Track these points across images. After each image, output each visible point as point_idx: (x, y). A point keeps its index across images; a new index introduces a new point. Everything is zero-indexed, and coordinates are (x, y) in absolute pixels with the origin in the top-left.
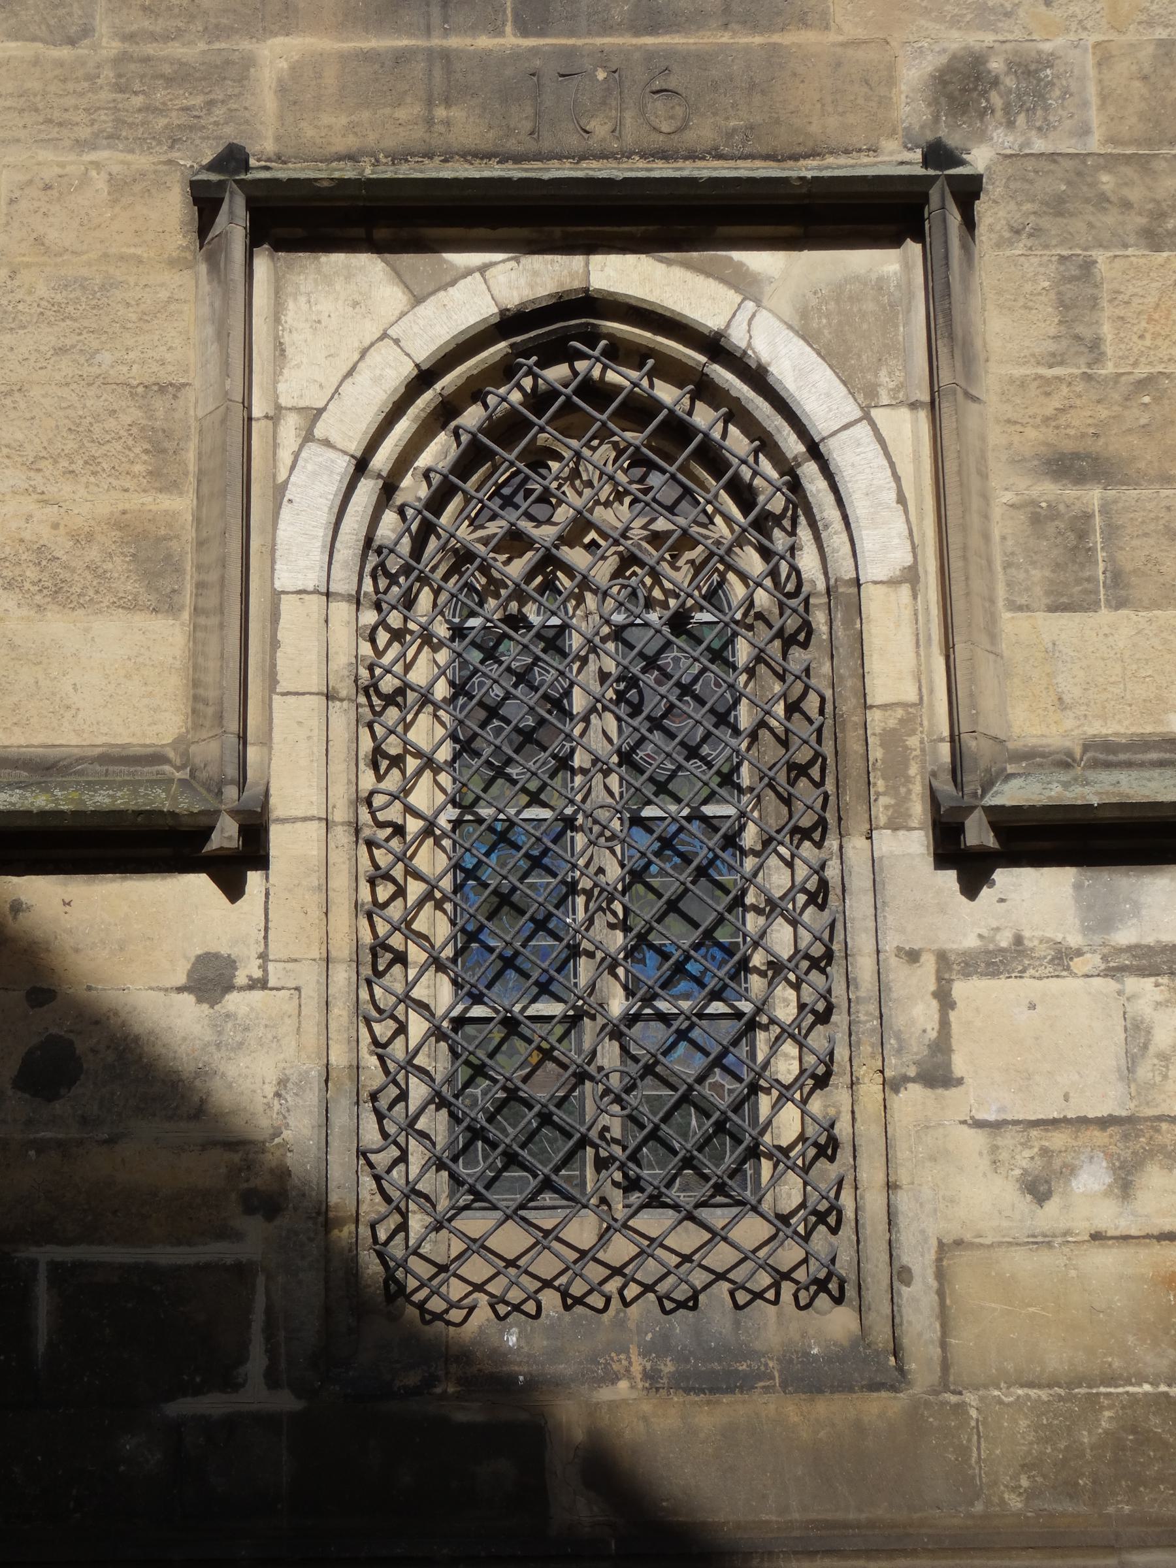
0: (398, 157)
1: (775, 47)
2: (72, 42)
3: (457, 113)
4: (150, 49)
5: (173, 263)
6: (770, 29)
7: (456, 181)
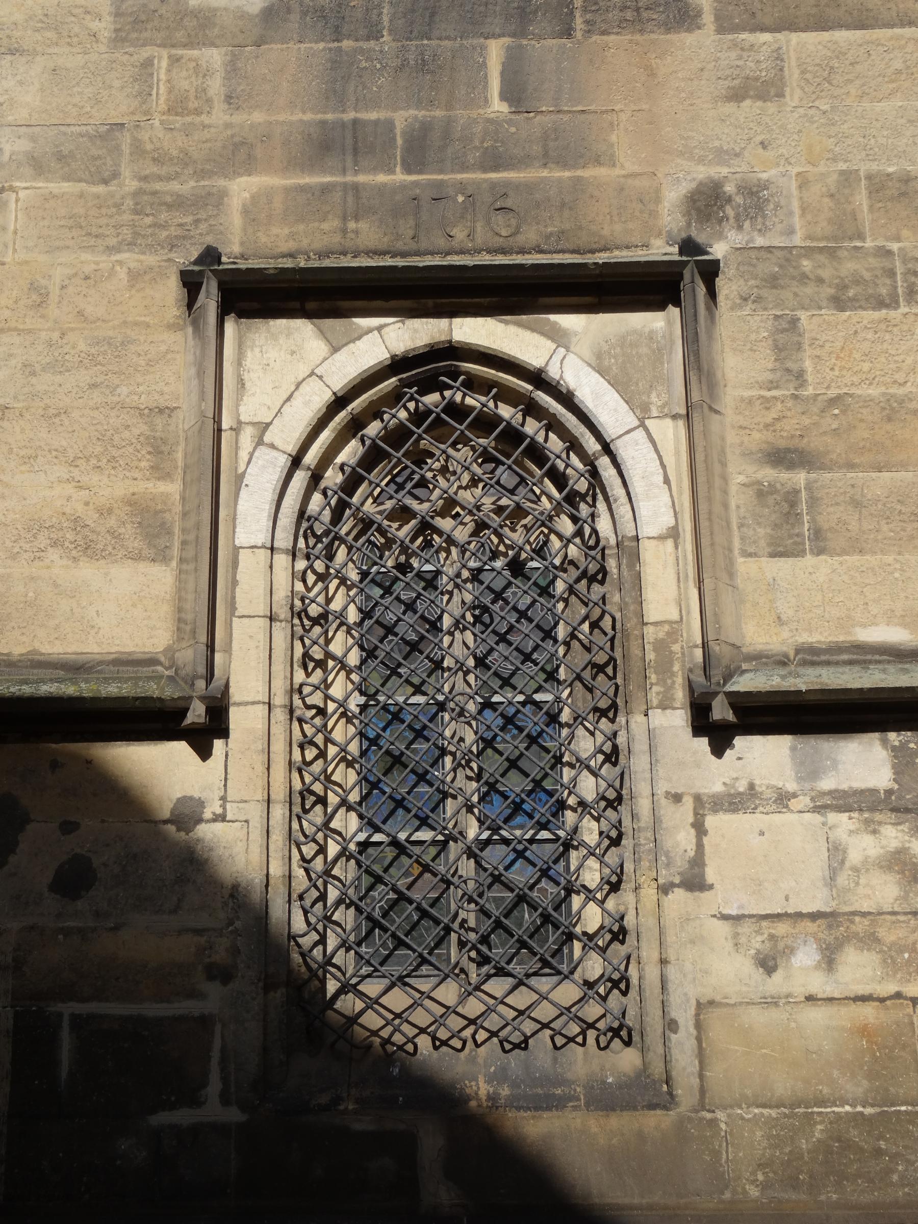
0: (321, 255)
1: (579, 179)
2: (105, 182)
3: (363, 225)
4: (158, 186)
5: (170, 327)
6: (574, 167)
7: (359, 269)
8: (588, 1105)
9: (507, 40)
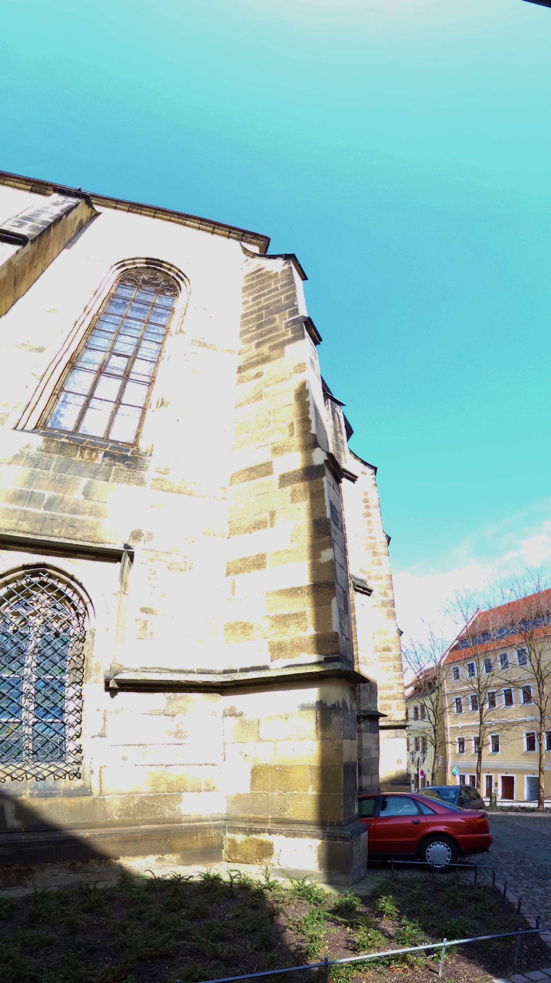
7: (17, 537)
8: (63, 796)
9: (90, 479)
